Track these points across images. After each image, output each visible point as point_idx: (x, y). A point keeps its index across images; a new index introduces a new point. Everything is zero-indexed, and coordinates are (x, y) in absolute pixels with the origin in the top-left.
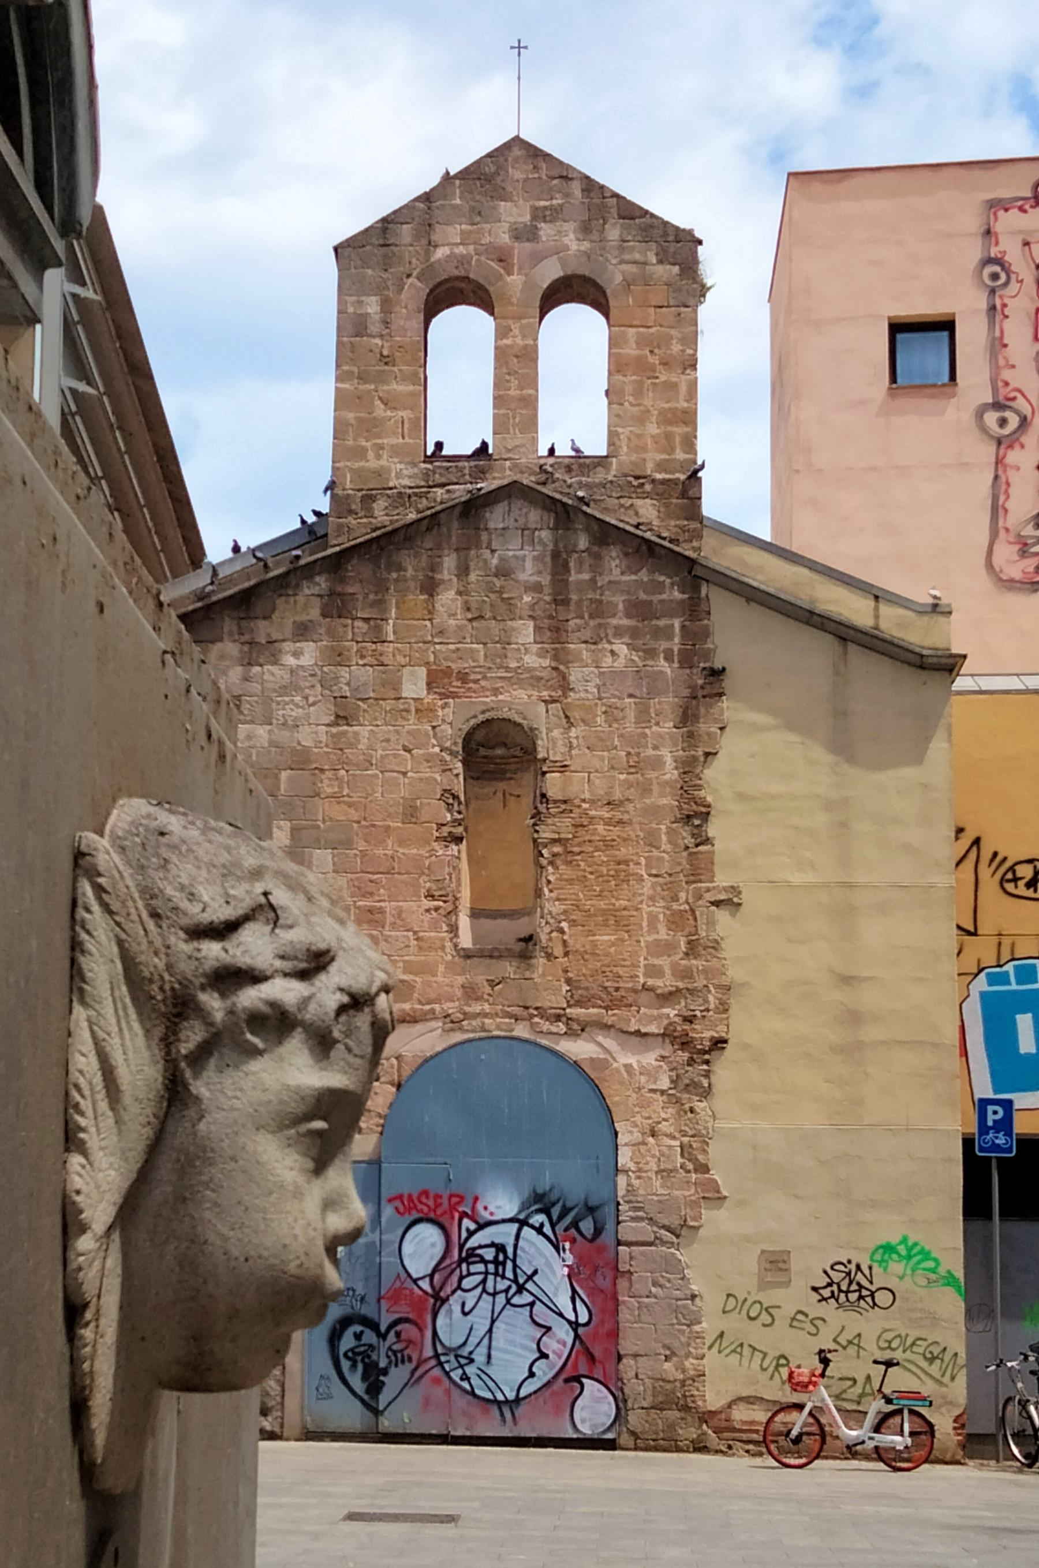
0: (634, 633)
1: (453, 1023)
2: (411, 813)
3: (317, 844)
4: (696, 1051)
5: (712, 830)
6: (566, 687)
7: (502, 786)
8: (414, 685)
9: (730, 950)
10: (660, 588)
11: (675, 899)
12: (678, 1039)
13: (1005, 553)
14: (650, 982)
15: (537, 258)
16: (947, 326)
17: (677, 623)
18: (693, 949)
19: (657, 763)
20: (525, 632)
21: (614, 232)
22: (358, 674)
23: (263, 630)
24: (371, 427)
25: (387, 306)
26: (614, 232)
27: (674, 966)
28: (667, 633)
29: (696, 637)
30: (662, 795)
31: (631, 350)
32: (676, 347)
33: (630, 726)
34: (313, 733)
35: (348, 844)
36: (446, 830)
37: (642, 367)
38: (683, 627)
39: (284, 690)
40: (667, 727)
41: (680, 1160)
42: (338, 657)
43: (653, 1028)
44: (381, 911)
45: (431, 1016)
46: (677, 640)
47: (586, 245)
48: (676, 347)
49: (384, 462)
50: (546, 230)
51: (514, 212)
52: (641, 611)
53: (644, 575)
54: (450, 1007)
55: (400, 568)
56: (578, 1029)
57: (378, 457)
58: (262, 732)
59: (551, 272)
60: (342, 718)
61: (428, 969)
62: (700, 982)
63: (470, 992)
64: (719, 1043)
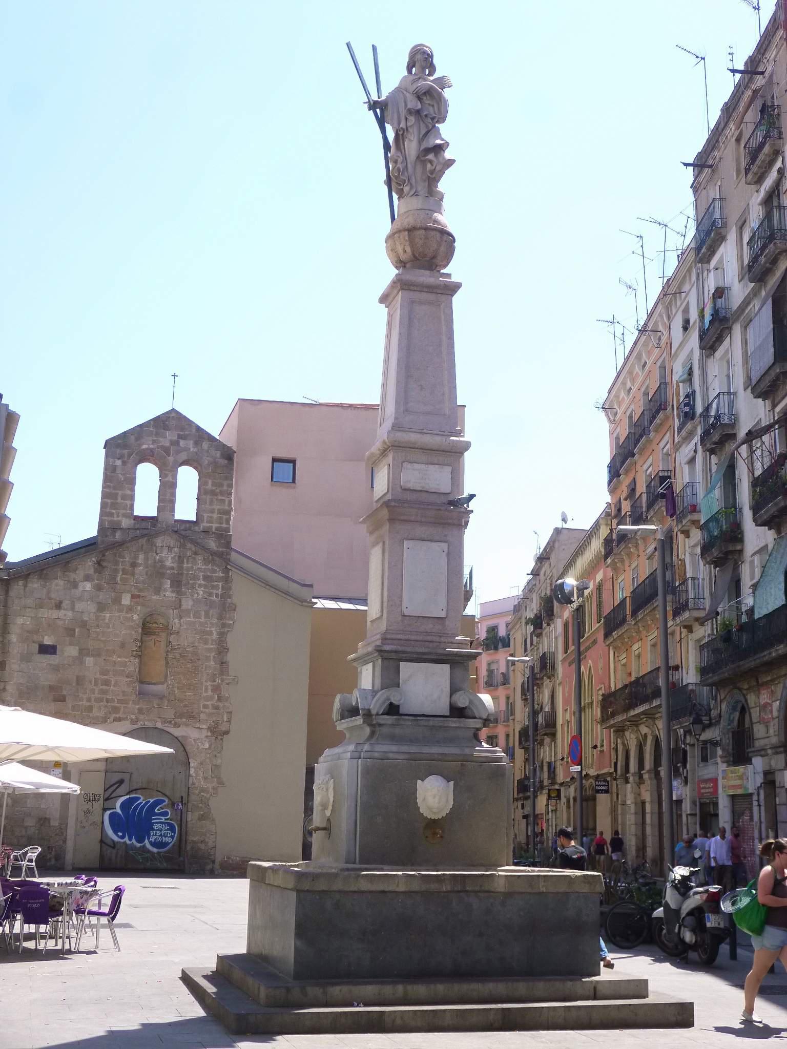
0: (205, 586)
1: (133, 722)
2: (123, 645)
3: (88, 655)
4: (218, 733)
5: (230, 657)
6: (180, 605)
7: (154, 637)
8: (126, 600)
10: (214, 571)
15: (178, 452)
16: (293, 462)
18: (220, 699)
19: (211, 633)
20: (167, 584)
21: (205, 445)
23: (72, 576)
24: (114, 505)
25: (124, 463)
26: (205, 445)
28: (217, 587)
29: (227, 589)
31: (209, 486)
32: (225, 488)
33: (202, 620)
35: (99, 655)
37: (213, 493)
39: (80, 599)
40: (215, 620)
42: (99, 588)
43: (204, 727)
45: (125, 719)
47: (195, 450)
48: (225, 488)
49: (120, 519)
50: (182, 443)
51: (171, 436)
53: (210, 567)
54: (133, 717)
55: (124, 557)
56: (177, 725)
57: (118, 516)
59: (183, 456)
63: (140, 711)
64: (227, 733)
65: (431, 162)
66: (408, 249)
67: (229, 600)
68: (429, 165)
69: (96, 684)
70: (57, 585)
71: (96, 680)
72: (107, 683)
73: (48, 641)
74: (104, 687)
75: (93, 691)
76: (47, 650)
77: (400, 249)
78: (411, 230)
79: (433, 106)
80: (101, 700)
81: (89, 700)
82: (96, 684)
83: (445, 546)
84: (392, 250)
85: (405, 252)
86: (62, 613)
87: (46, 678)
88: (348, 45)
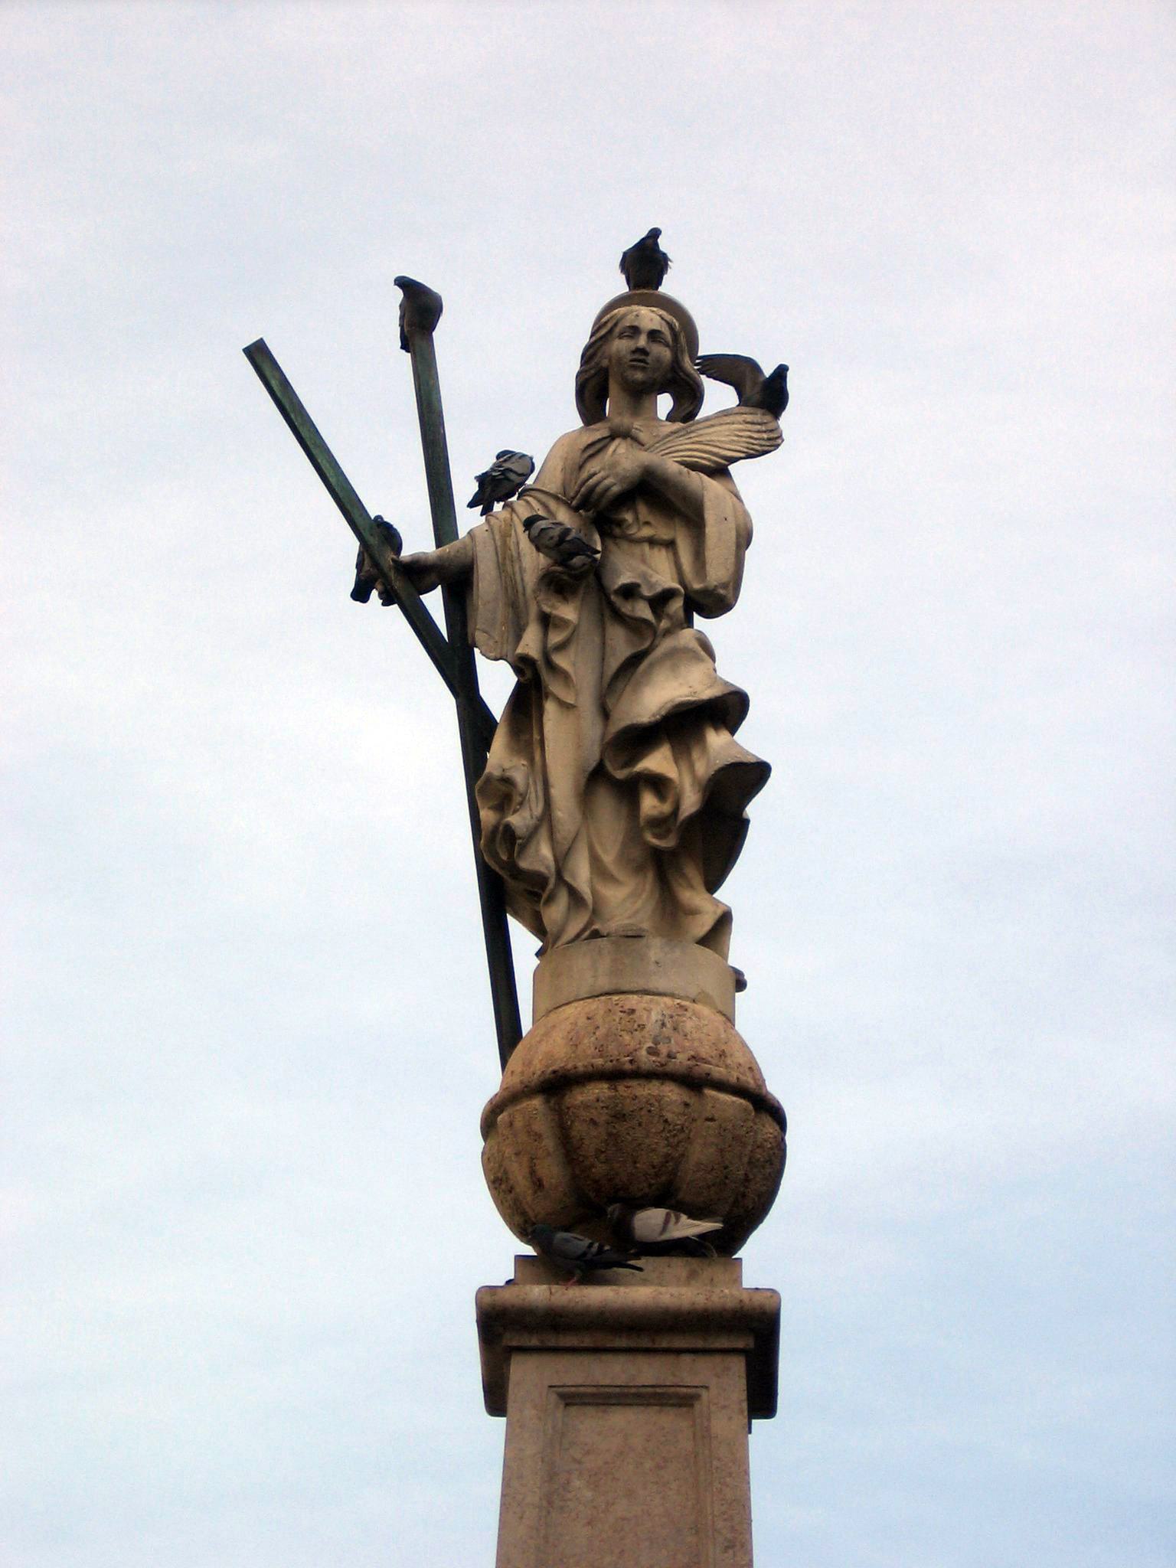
65: (658, 784)
66: (552, 1171)
68: (649, 804)
77: (519, 1175)
78: (556, 1085)
79: (670, 545)
84: (499, 1183)
85: (538, 1184)
88: (259, 355)
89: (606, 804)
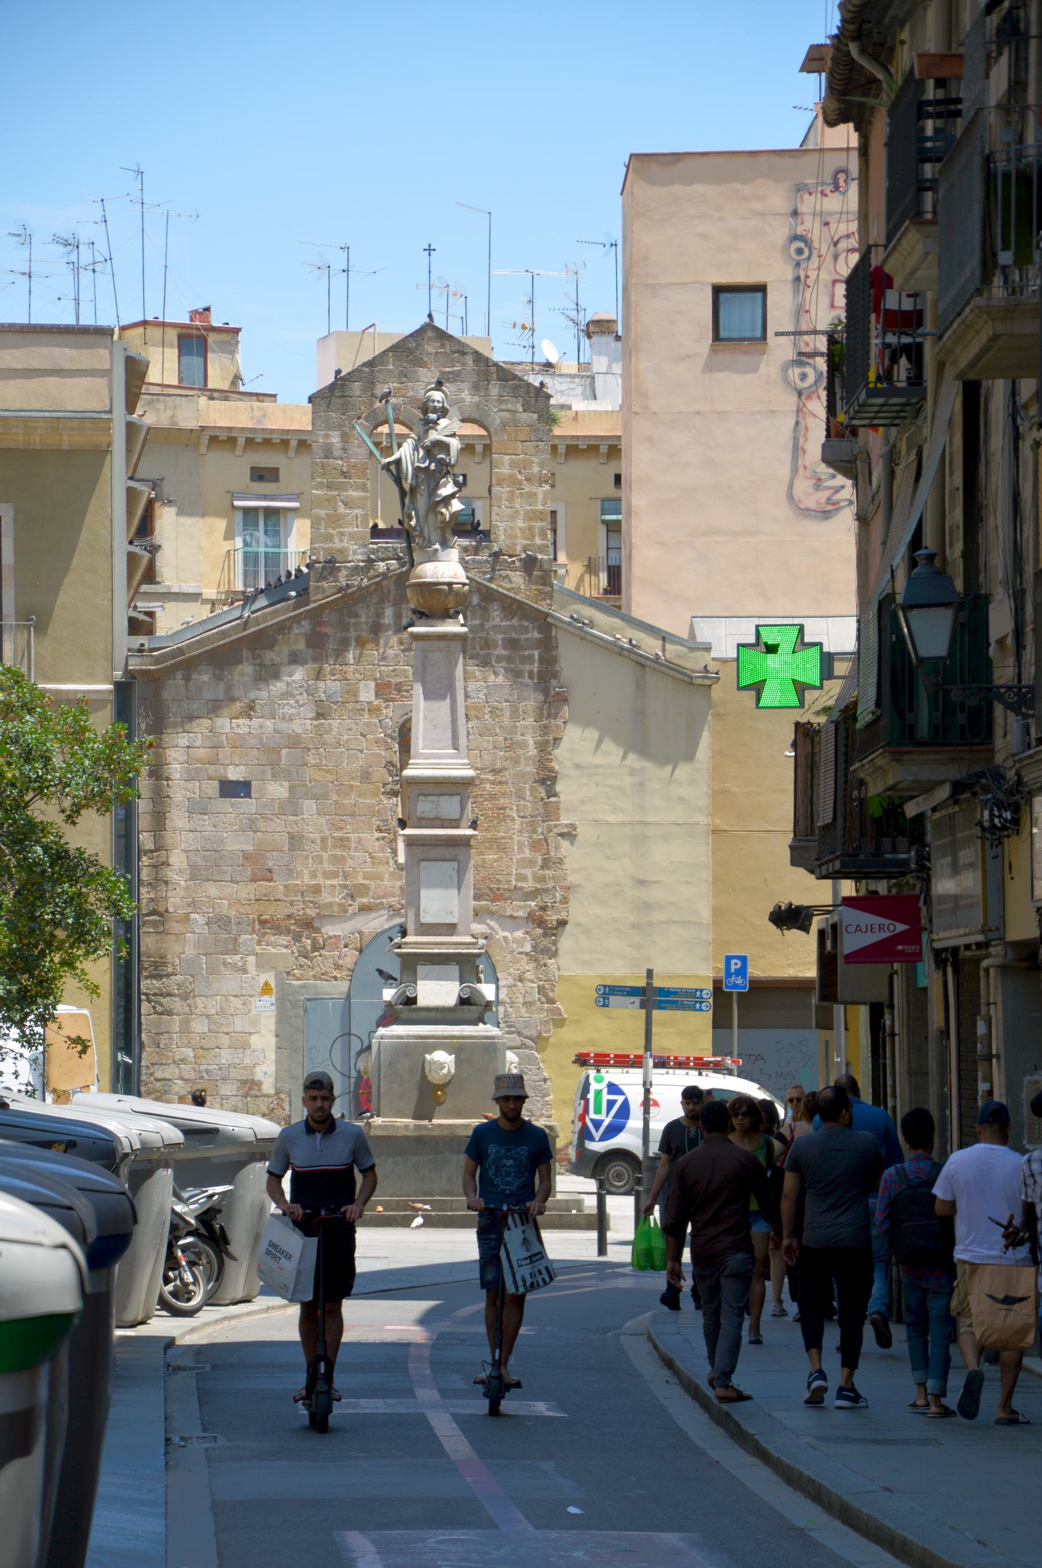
0: (509, 659)
2: (366, 776)
3: (306, 796)
5: (558, 788)
8: (367, 693)
9: (569, 864)
10: (526, 630)
11: (535, 831)
12: (536, 920)
13: (803, 486)
14: (519, 884)
17: (536, 653)
18: (546, 864)
19: (524, 745)
21: (494, 390)
22: (330, 686)
23: (269, 656)
25: (345, 438)
26: (494, 390)
27: (534, 873)
28: (529, 659)
30: (527, 765)
33: (506, 721)
34: (303, 725)
36: (389, 787)
38: (540, 656)
41: (537, 996)
43: (521, 914)
44: (348, 839)
45: (379, 907)
46: (536, 665)
48: (536, 469)
49: (346, 545)
52: (513, 644)
53: (515, 621)
54: (392, 900)
55: (357, 615)
57: (341, 541)
58: (269, 723)
60: (319, 716)
61: (379, 877)
62: (550, 884)
64: (563, 923)
67: (554, 682)
69: (324, 848)
70: (242, 675)
71: (324, 840)
72: (343, 843)
73: (234, 774)
74: (338, 852)
75: (319, 859)
76: (234, 789)
80: (334, 875)
81: (314, 876)
82: (324, 848)
83: (455, 864)
86: (256, 722)
87: (236, 844)
89: (431, 516)
